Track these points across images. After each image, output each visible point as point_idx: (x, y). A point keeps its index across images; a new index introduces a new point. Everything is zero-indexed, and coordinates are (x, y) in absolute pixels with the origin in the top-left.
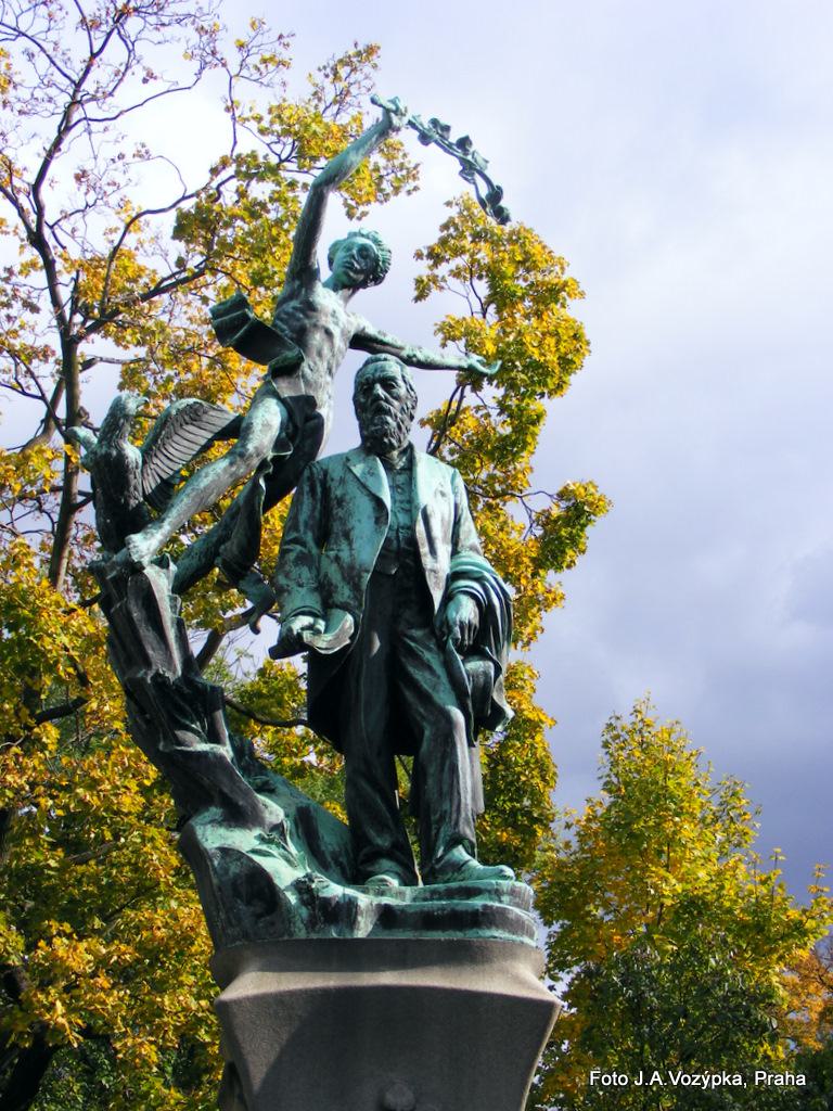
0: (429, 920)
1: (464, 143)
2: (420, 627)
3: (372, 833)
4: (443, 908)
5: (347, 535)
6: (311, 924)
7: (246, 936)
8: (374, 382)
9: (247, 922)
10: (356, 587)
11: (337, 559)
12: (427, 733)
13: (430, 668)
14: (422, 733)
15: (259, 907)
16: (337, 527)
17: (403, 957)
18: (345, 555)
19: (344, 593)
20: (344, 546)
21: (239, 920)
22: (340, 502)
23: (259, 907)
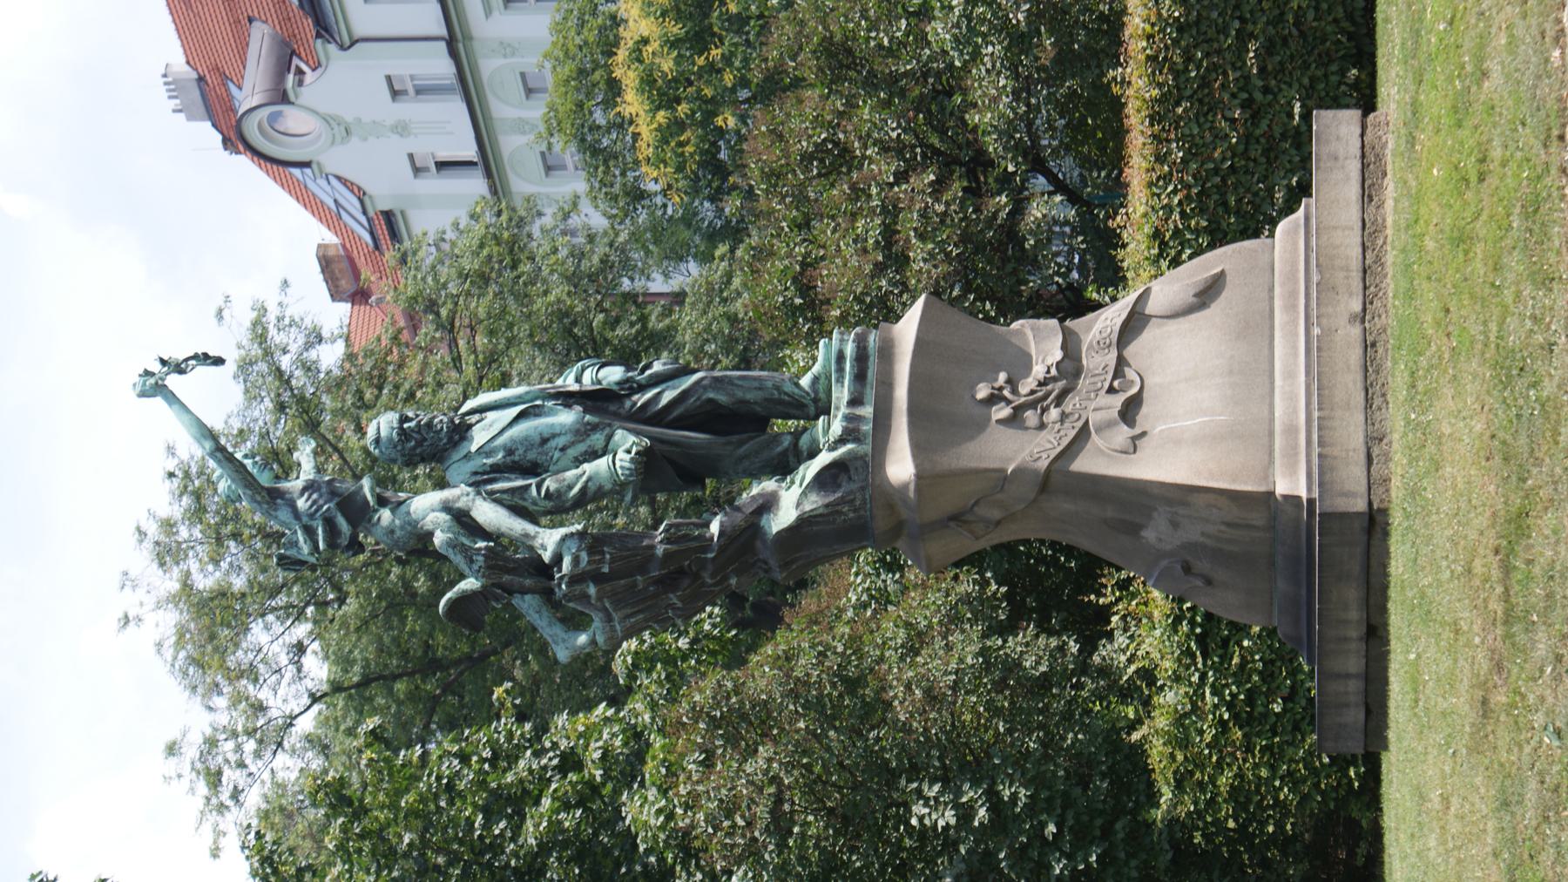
0: (860, 377)
1: (163, 362)
2: (623, 403)
3: (779, 449)
4: (852, 367)
5: (544, 441)
6: (857, 440)
7: (863, 489)
8: (401, 428)
9: (854, 486)
10: (594, 428)
11: (563, 449)
12: (711, 395)
13: (659, 394)
14: (710, 401)
15: (843, 478)
16: (531, 456)
17: (887, 384)
18: (561, 441)
19: (597, 439)
20: (553, 443)
21: (852, 492)
22: (510, 452)
23: (843, 478)
